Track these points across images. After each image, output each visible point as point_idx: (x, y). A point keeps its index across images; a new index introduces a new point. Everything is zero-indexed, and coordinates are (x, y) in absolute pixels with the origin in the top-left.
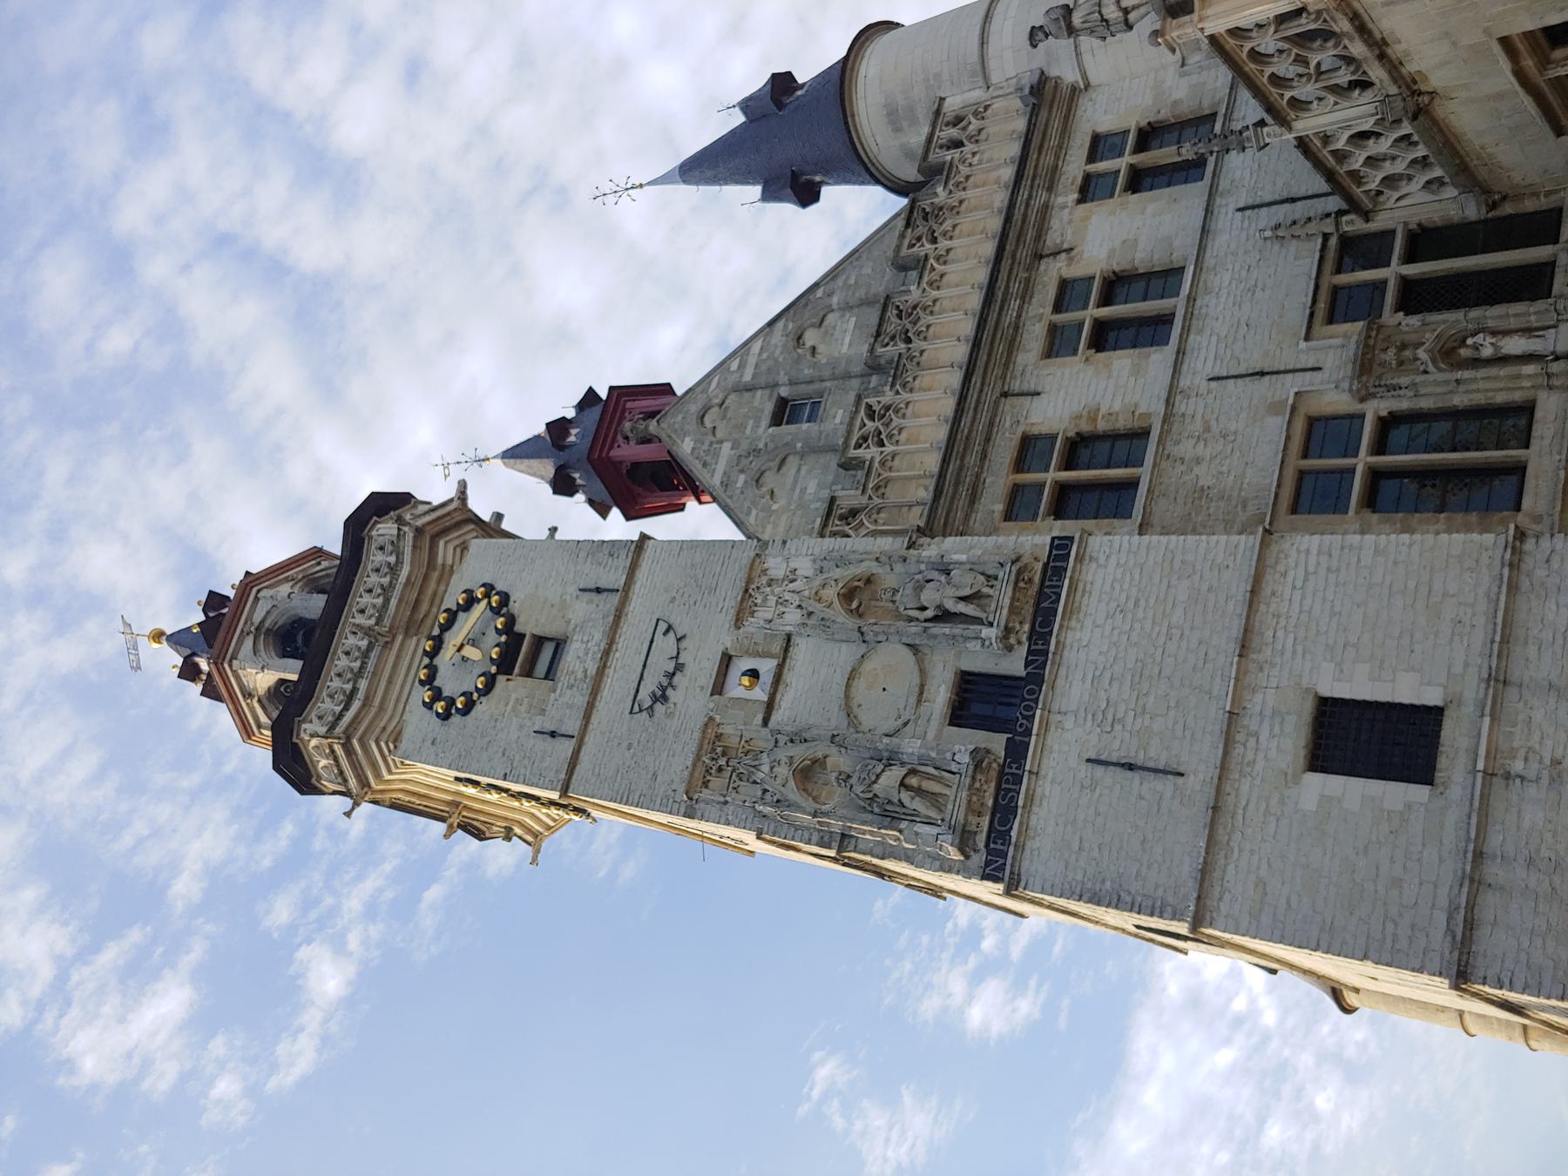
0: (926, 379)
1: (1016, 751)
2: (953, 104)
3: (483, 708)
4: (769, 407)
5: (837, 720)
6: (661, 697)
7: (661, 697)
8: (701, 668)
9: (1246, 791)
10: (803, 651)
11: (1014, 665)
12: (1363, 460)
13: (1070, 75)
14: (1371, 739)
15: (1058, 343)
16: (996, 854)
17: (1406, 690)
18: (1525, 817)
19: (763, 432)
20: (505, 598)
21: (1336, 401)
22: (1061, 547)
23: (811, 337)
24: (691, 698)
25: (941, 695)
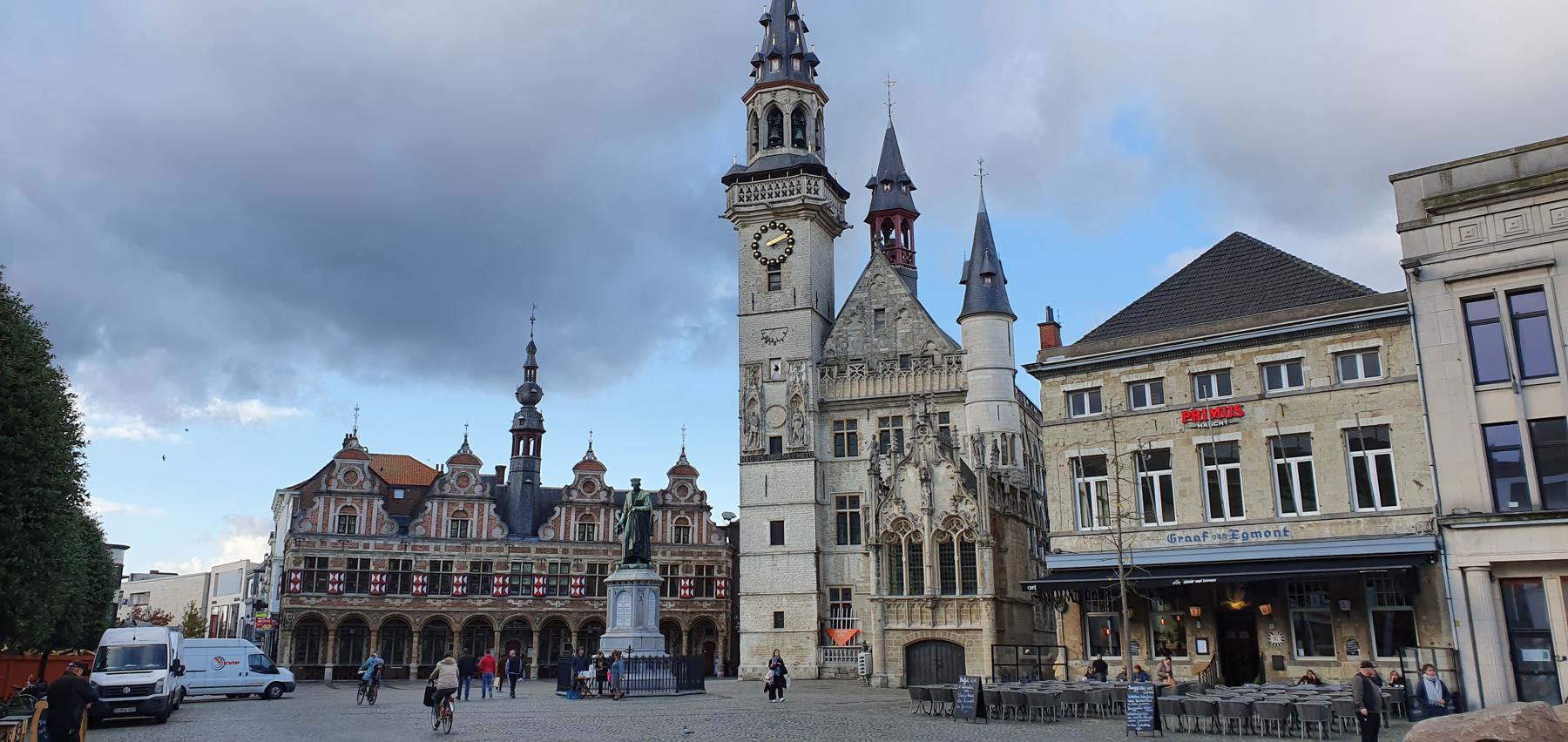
0: (871, 382)
1: (766, 458)
2: (964, 359)
3: (757, 262)
4: (881, 306)
5: (768, 404)
6: (767, 340)
7: (767, 340)
8: (773, 351)
9: (765, 510)
10: (783, 386)
11: (785, 451)
12: (848, 511)
13: (968, 399)
14: (777, 533)
15: (883, 421)
16: (747, 459)
17: (786, 537)
18: (767, 561)
19: (870, 312)
20: (790, 253)
21: (862, 502)
22: (809, 455)
23: (905, 313)
24: (768, 351)
25: (775, 434)
